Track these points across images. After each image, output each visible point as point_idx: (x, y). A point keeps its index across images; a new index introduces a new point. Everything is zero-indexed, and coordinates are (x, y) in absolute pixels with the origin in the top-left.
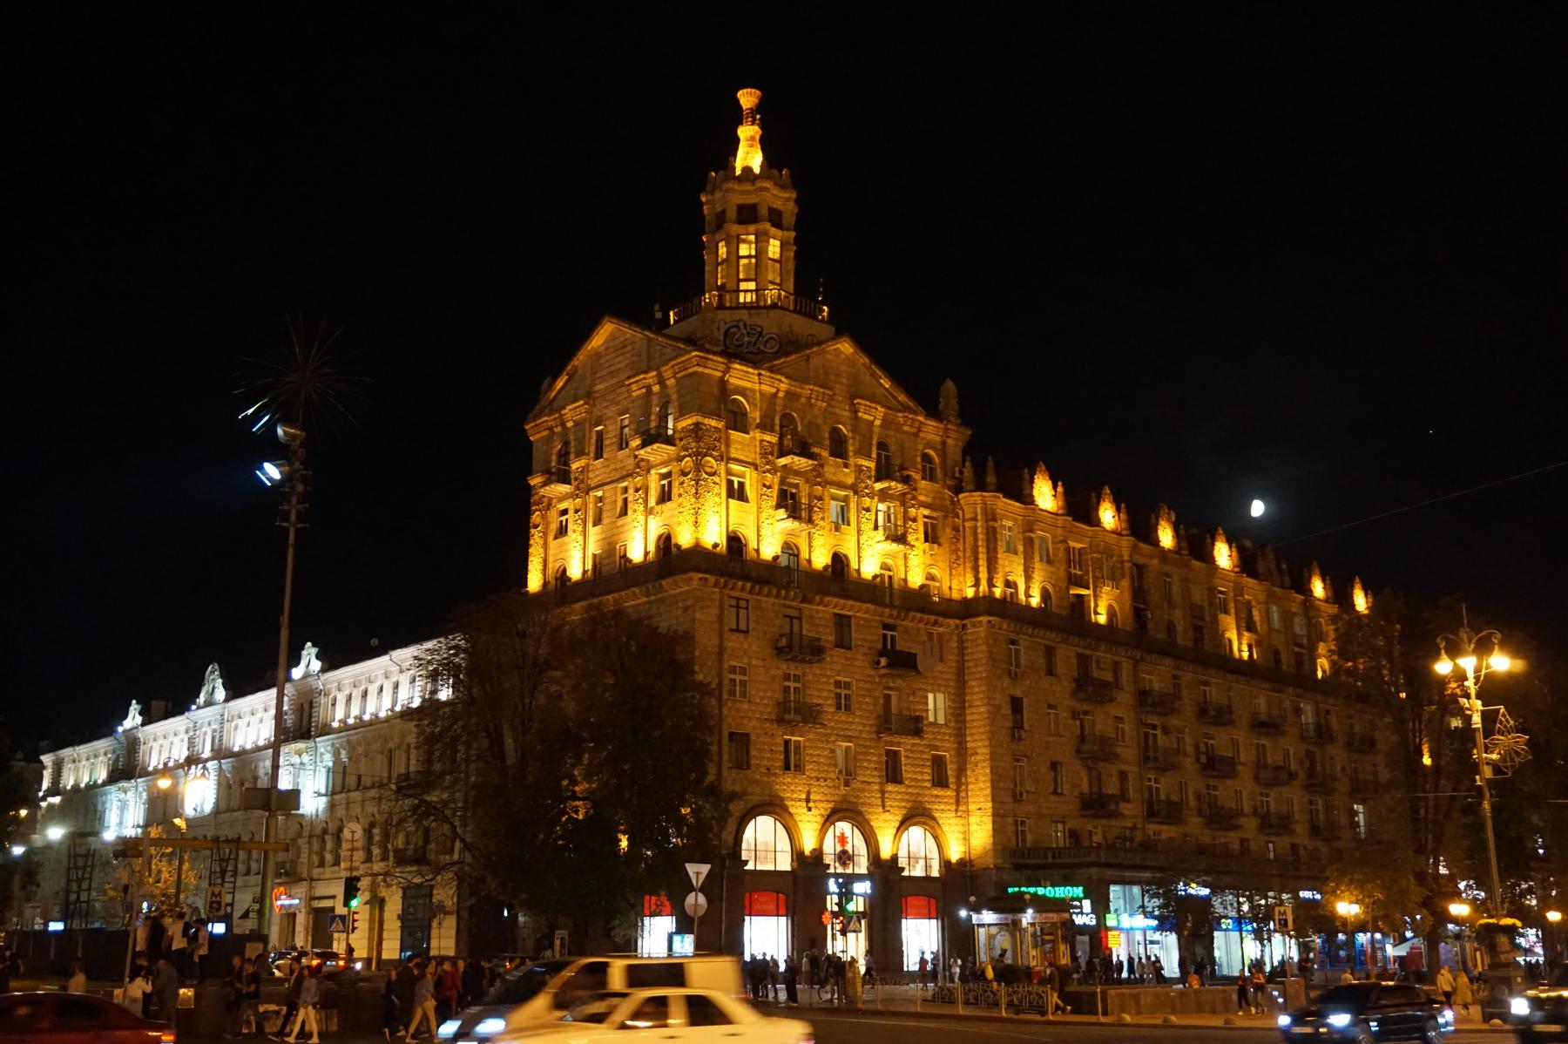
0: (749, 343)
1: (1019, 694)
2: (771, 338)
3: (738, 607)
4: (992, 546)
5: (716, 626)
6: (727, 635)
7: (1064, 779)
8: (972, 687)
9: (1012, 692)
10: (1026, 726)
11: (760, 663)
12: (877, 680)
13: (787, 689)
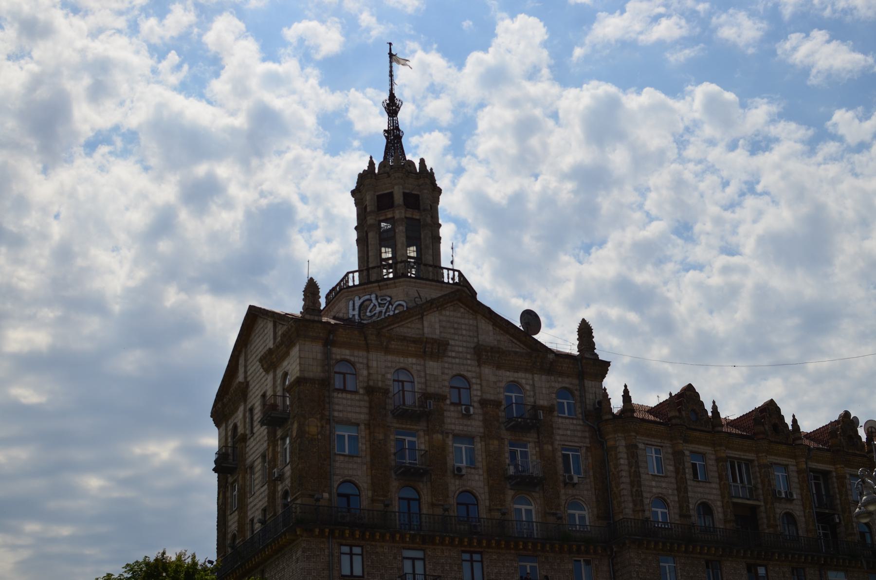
0: (381, 312)
2: (400, 305)
3: (351, 554)
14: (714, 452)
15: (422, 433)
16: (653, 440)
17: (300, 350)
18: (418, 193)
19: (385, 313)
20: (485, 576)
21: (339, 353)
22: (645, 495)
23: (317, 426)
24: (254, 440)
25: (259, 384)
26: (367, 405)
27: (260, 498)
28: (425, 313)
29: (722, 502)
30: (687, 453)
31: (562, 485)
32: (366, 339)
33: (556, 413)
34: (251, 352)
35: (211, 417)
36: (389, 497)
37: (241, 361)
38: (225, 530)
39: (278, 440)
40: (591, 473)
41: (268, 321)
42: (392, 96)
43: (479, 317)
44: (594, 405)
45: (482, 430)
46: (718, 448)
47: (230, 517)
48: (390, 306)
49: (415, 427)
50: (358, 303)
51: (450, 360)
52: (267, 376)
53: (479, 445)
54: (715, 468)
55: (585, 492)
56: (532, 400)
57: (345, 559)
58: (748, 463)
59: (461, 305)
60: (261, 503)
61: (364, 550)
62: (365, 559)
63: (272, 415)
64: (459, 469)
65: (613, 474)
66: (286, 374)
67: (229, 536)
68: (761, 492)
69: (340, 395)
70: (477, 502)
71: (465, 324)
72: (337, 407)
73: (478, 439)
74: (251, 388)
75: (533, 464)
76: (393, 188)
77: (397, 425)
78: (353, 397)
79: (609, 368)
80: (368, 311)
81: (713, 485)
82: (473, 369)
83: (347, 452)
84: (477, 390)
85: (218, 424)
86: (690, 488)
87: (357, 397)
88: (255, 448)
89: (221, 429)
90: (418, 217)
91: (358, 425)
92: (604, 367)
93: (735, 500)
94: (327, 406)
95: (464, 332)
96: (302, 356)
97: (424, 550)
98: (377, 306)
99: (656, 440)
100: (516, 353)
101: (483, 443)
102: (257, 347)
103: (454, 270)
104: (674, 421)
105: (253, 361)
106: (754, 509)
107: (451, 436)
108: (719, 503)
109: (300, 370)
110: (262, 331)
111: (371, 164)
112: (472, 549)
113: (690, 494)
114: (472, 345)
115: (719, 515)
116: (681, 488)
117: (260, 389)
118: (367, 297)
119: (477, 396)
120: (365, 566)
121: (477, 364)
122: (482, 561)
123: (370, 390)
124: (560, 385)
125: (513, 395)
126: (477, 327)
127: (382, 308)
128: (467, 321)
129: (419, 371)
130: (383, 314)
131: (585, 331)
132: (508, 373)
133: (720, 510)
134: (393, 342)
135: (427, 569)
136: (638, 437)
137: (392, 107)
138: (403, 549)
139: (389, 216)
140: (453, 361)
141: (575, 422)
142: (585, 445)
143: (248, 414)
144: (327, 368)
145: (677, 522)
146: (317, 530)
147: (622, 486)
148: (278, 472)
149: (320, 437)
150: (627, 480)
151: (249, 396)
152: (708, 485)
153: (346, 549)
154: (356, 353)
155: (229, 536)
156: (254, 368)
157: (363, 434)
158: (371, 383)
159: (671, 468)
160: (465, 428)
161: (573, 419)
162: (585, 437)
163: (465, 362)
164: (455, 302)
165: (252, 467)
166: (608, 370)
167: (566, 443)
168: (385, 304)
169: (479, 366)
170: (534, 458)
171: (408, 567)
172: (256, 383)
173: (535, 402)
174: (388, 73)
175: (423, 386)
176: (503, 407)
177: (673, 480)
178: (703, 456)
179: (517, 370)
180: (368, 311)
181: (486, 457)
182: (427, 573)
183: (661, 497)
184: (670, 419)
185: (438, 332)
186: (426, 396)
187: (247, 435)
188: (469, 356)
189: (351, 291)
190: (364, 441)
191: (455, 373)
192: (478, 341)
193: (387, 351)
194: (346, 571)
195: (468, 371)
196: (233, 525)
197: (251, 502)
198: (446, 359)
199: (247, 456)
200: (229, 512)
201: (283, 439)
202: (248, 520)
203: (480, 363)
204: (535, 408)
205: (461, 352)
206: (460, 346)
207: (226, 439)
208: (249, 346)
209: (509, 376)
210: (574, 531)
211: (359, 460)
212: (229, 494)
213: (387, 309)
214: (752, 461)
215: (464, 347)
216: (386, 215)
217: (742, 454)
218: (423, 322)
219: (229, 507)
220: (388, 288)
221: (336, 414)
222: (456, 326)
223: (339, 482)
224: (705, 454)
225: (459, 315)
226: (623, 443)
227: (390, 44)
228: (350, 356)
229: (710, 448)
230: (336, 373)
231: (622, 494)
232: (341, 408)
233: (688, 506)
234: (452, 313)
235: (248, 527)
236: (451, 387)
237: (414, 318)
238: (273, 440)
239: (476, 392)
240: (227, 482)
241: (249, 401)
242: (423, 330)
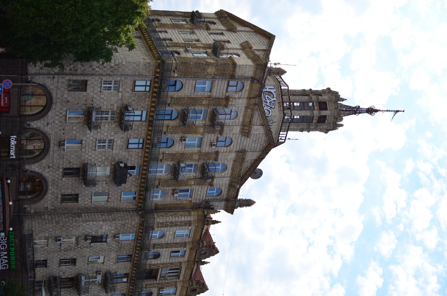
0: (267, 102)
1: (108, 240)
2: (270, 112)
3: (146, 86)
4: (179, 223)
5: (137, 74)
6: (133, 79)
7: (67, 266)
8: (111, 215)
9: (109, 236)
10: (92, 244)
11: (120, 97)
12: (113, 163)
13: (107, 113)
14: (184, 261)
15: (204, 122)
16: (193, 233)
17: (250, 65)
18: (326, 123)
19: (266, 105)
20: (131, 150)
21: (247, 84)
22: (166, 228)
23: (211, 72)
24: (207, 35)
25: (235, 39)
26: (220, 97)
27: (177, 37)
28: (264, 127)
29: (160, 264)
30: (185, 249)
31: (174, 188)
32: (254, 98)
33: (209, 187)
34: (252, 35)
35: (220, 10)
36: (173, 106)
37: (248, 29)
38: (163, 15)
39: (206, 49)
40: (178, 202)
41: (266, 46)
42: (377, 111)
43: (260, 153)
44: (212, 206)
45: (204, 151)
46: (186, 263)
47: (169, 18)
48: (269, 108)
49: (207, 120)
50: (272, 91)
51: (240, 137)
52: (239, 44)
53: (196, 149)
54: (176, 261)
55: (169, 199)
56: (217, 176)
57: (143, 83)
58: (178, 277)
59: (267, 144)
60: (174, 38)
61: (147, 92)
62: (143, 92)
63: (218, 49)
64: (185, 140)
65: (177, 214)
66: (238, 55)
67: (159, 18)
68: (164, 281)
69: (226, 84)
70: (168, 147)
71: (257, 146)
72: (220, 82)
73: (199, 149)
74: (233, 34)
75: (184, 175)
76: (329, 111)
77: (209, 111)
78: (225, 90)
79: (230, 214)
80: (268, 96)
81: (168, 260)
82: (235, 149)
83: (197, 86)
84: (224, 150)
85: (217, 13)
86: (167, 249)
87: (224, 92)
88: (203, 35)
89: (214, 15)
90: (313, 122)
91: (210, 92)
92: (230, 210)
93: (160, 270)
94: (221, 77)
95: (253, 145)
96: (247, 66)
97: (146, 121)
98: (270, 101)
99: (192, 235)
100: (241, 170)
101: (197, 152)
102: (254, 38)
103: (285, 140)
104: (201, 244)
105: (247, 36)
106: (155, 278)
107: (202, 136)
108: (159, 262)
109: (240, 65)
110: (262, 42)
111: (343, 100)
112: (144, 144)
113: (164, 249)
114: (246, 149)
115: (154, 262)
116: (167, 245)
117: (232, 40)
118: (275, 96)
119: (221, 150)
120: (139, 93)
121: (237, 150)
122: (138, 148)
123: (227, 99)
124: (223, 190)
125: (220, 167)
126: (256, 151)
127: (269, 103)
128: (259, 147)
129: (235, 122)
130: (266, 104)
131: (249, 203)
132: (231, 165)
133: (156, 262)
134: (251, 110)
135: (136, 122)
136: (194, 226)
137: (371, 111)
138: (147, 111)
139: (315, 108)
140: (239, 139)
141: (205, 196)
142: (193, 200)
143: (220, 31)
144: (240, 78)
145: (151, 242)
146: (159, 70)
147: (171, 217)
148: (189, 50)
149: (206, 73)
150: (174, 220)
152: (169, 257)
153: (148, 83)
154: (247, 92)
155: (159, 18)
156: (244, 36)
157: (206, 94)
158: (231, 99)
159: (178, 241)
160: (205, 144)
161: (206, 195)
162: (196, 200)
163: (238, 145)
164: (268, 141)
165: (193, 33)
166: (229, 213)
167: (194, 191)
168: (271, 105)
169: (236, 152)
170: (188, 176)
171: (137, 113)
172: (236, 37)
173: (216, 177)
174: (388, 109)
175: (227, 124)
176: (214, 162)
177: (172, 242)
178: (183, 256)
179: (233, 170)
180: (268, 96)
181: (190, 153)
182: (134, 122)
183: (164, 235)
184: (202, 242)
185: (255, 132)
186: (222, 126)
187: (210, 30)
188: (241, 147)
189: (278, 88)
190: (202, 94)
191: (233, 140)
192: (248, 152)
193: (247, 108)
194: (138, 83)
195: (234, 146)
196: (165, 20)
197: (175, 32)
198: (240, 136)
199: (199, 30)
200: (171, 18)
201: (206, 53)
202: (167, 30)
203: (238, 152)
204: (213, 178)
205: (243, 143)
206: (246, 143)
207: (208, 18)
208: (255, 33)
209: (230, 166)
210: (150, 194)
211: (193, 92)
212: (180, 18)
213: (268, 106)
214: (179, 278)
215: (246, 145)
216: (316, 106)
217: (183, 274)
218: (260, 125)
219: (174, 18)
220: (279, 107)
221: (217, 81)
222: (257, 141)
223: (182, 81)
224: (184, 257)
225: (262, 143)
226: (192, 219)
227: (404, 111)
228: (246, 90)
229: (186, 259)
230: (237, 82)
231: (167, 217)
232: (220, 84)
233: (159, 248)
234: (263, 139)
235: (163, 30)
236: (226, 138)
237: (262, 121)
238: (206, 47)
239: (222, 149)
240: (186, 17)
241: (226, 32)
242: (256, 125)
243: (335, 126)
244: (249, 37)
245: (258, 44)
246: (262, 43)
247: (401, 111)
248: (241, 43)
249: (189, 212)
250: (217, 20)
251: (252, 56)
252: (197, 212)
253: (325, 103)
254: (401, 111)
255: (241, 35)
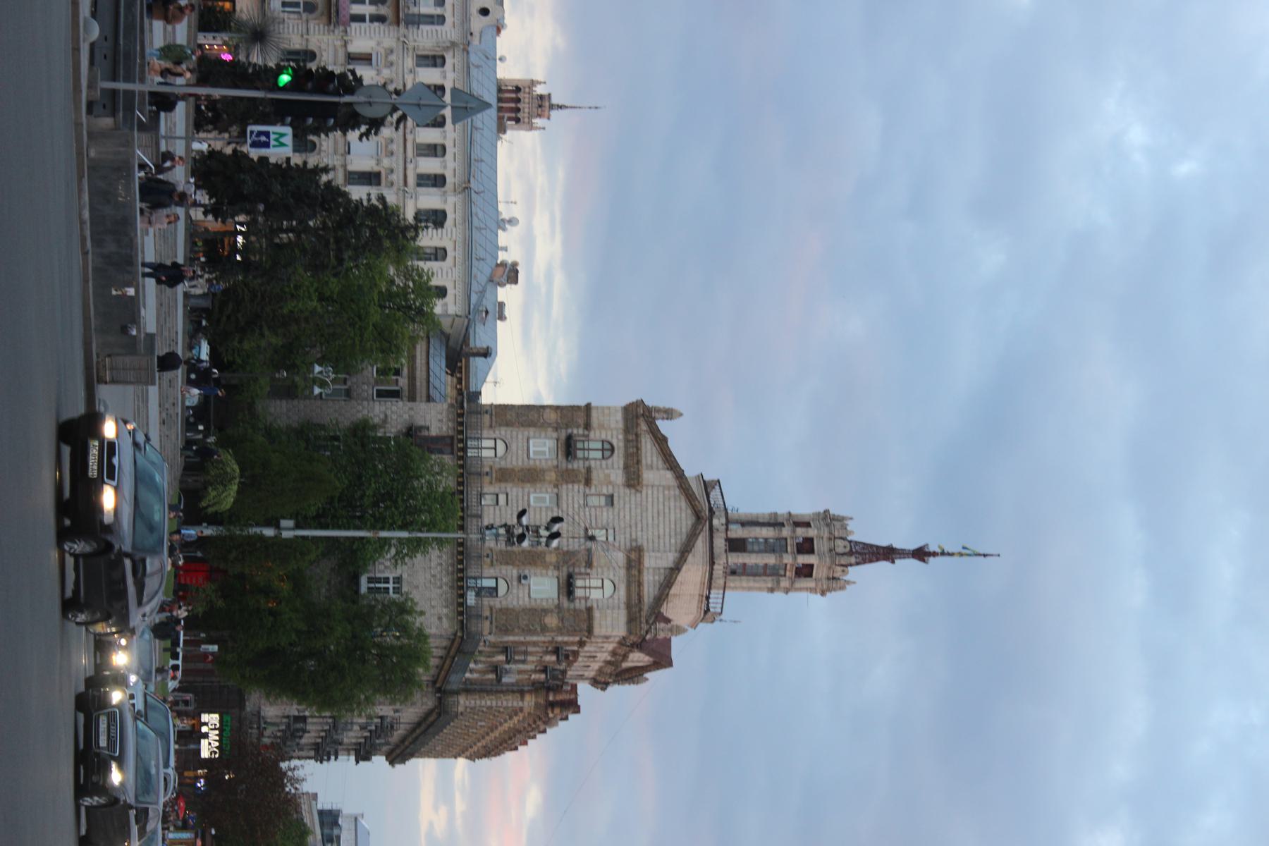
39: (558, 569)
42: (934, 554)
89: (619, 416)
110: (678, 530)
137: (921, 554)
139: (788, 573)
151: (627, 491)
172: (633, 511)
202: (508, 490)
208: (677, 491)
241: (622, 490)
243: (833, 583)
244: (661, 507)
245: (667, 537)
246: (676, 534)
247: (992, 555)
248: (634, 537)
249: (522, 693)
250: (621, 437)
251: (635, 597)
252: (536, 697)
253: (811, 566)
254: (992, 555)
255: (647, 502)
